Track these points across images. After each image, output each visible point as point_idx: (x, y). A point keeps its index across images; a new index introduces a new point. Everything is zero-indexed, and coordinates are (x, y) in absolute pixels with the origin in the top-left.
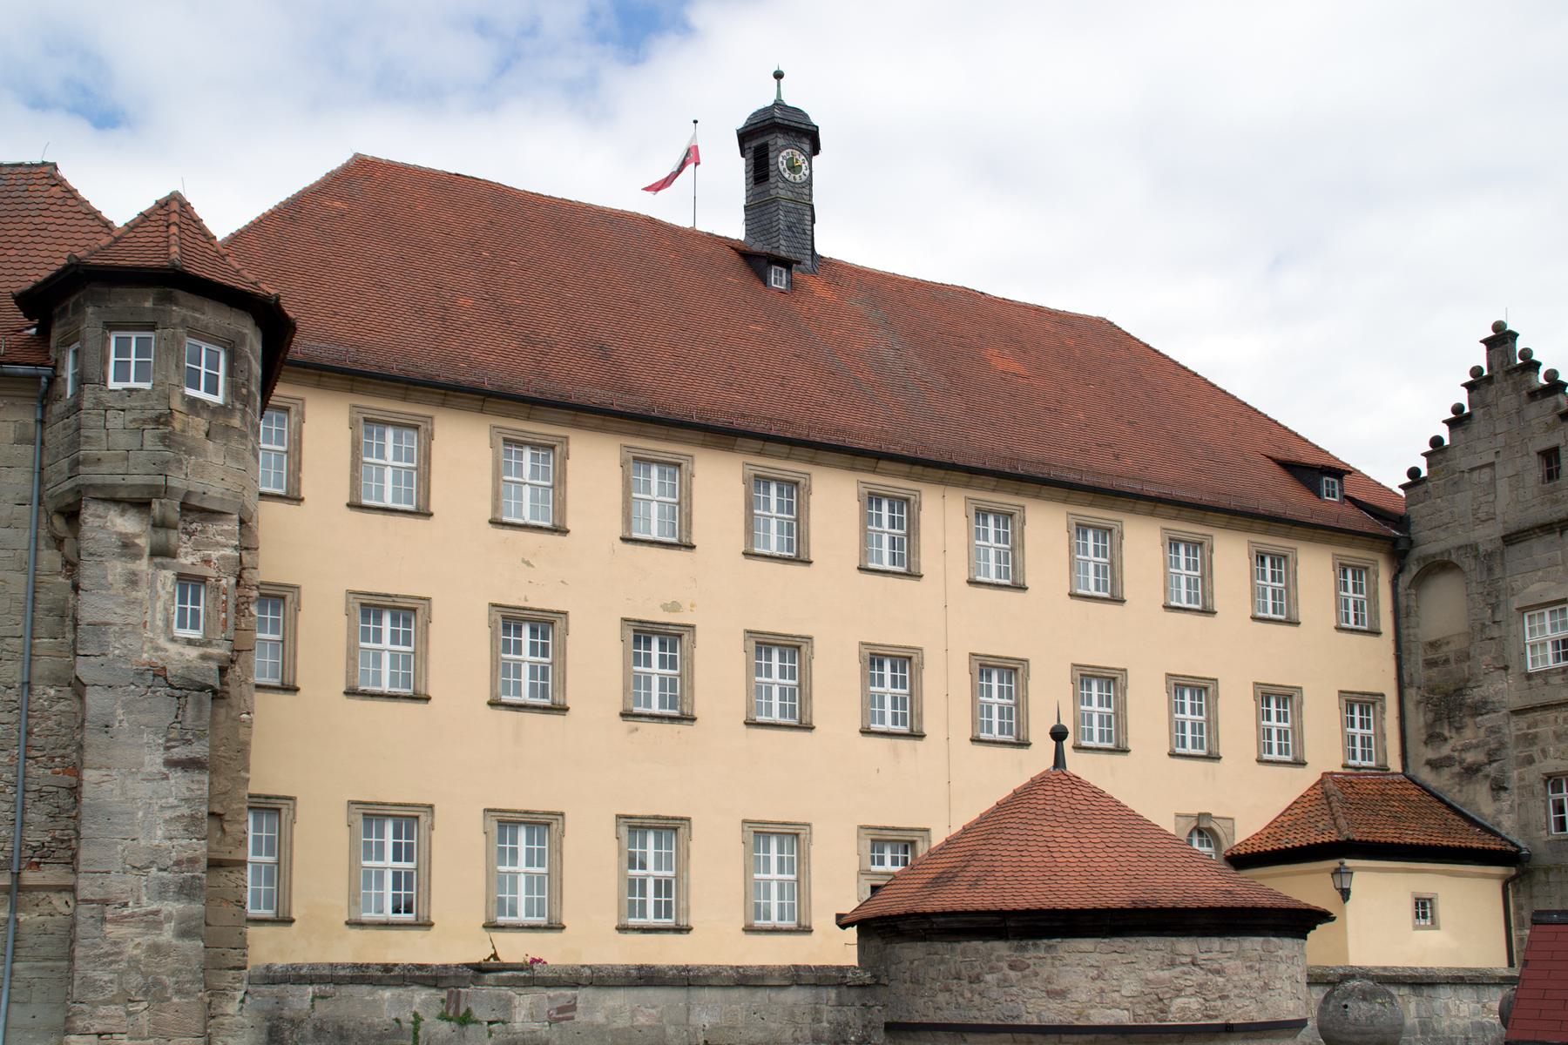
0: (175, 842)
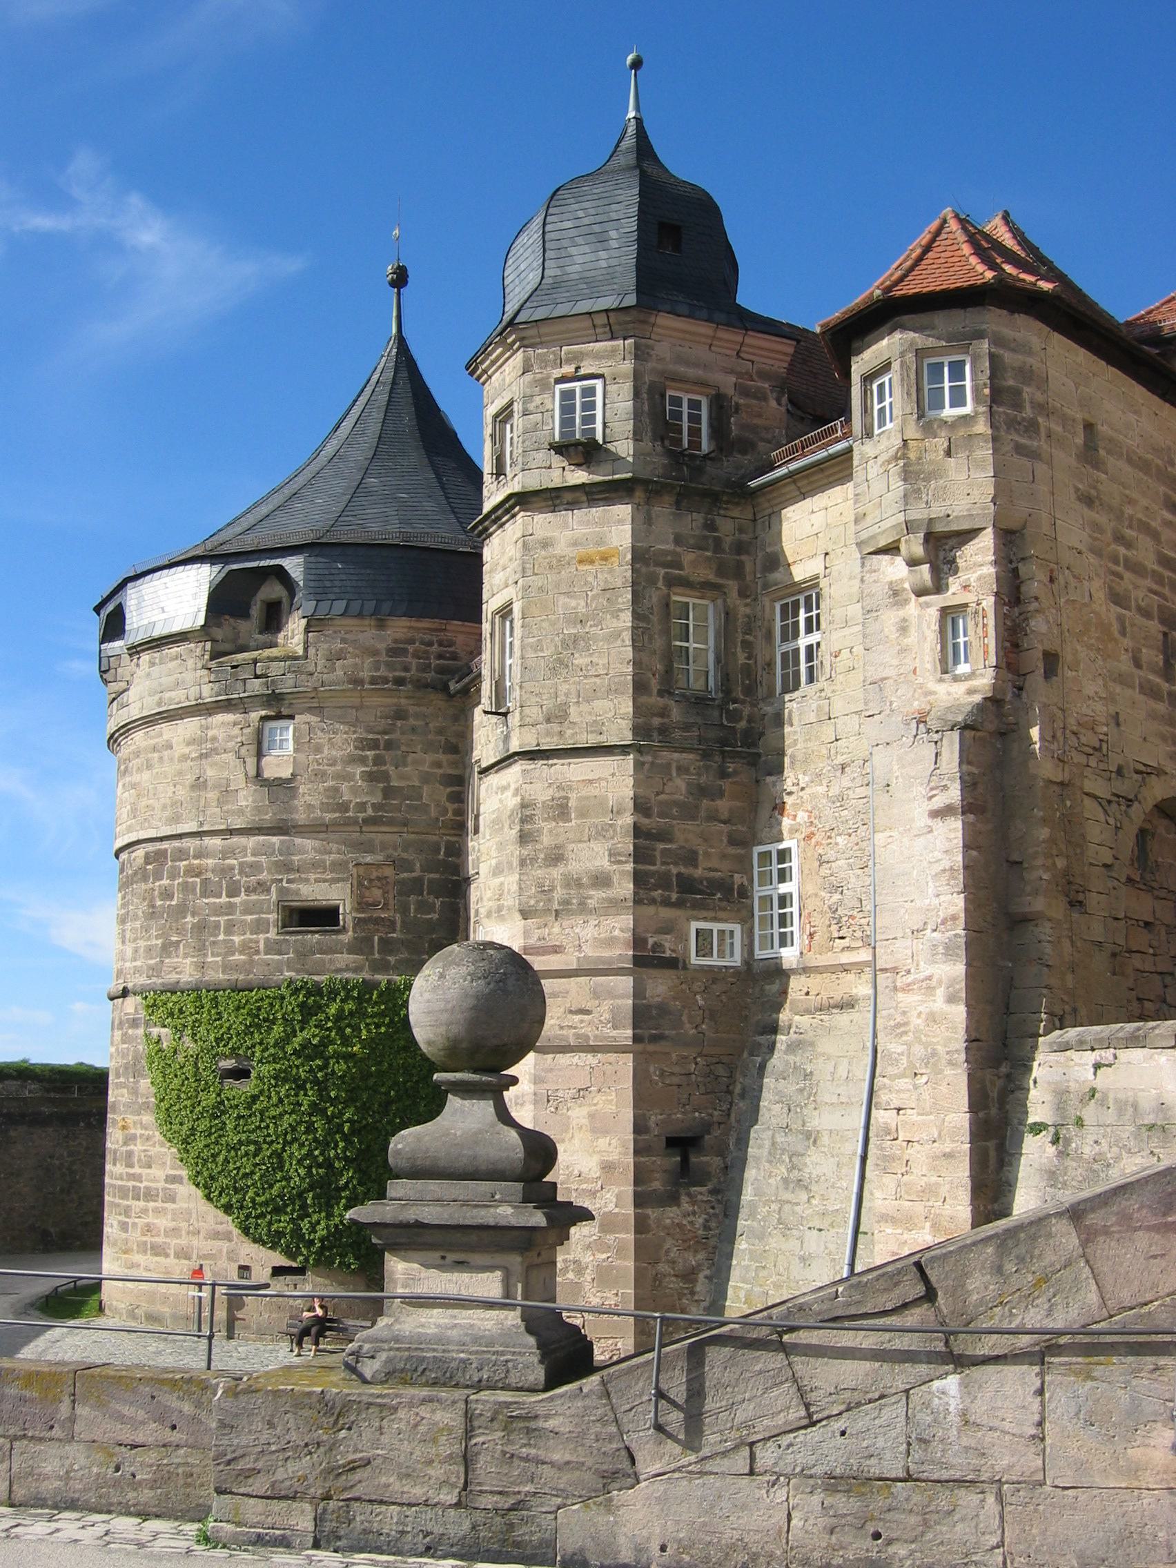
0: (942, 898)
